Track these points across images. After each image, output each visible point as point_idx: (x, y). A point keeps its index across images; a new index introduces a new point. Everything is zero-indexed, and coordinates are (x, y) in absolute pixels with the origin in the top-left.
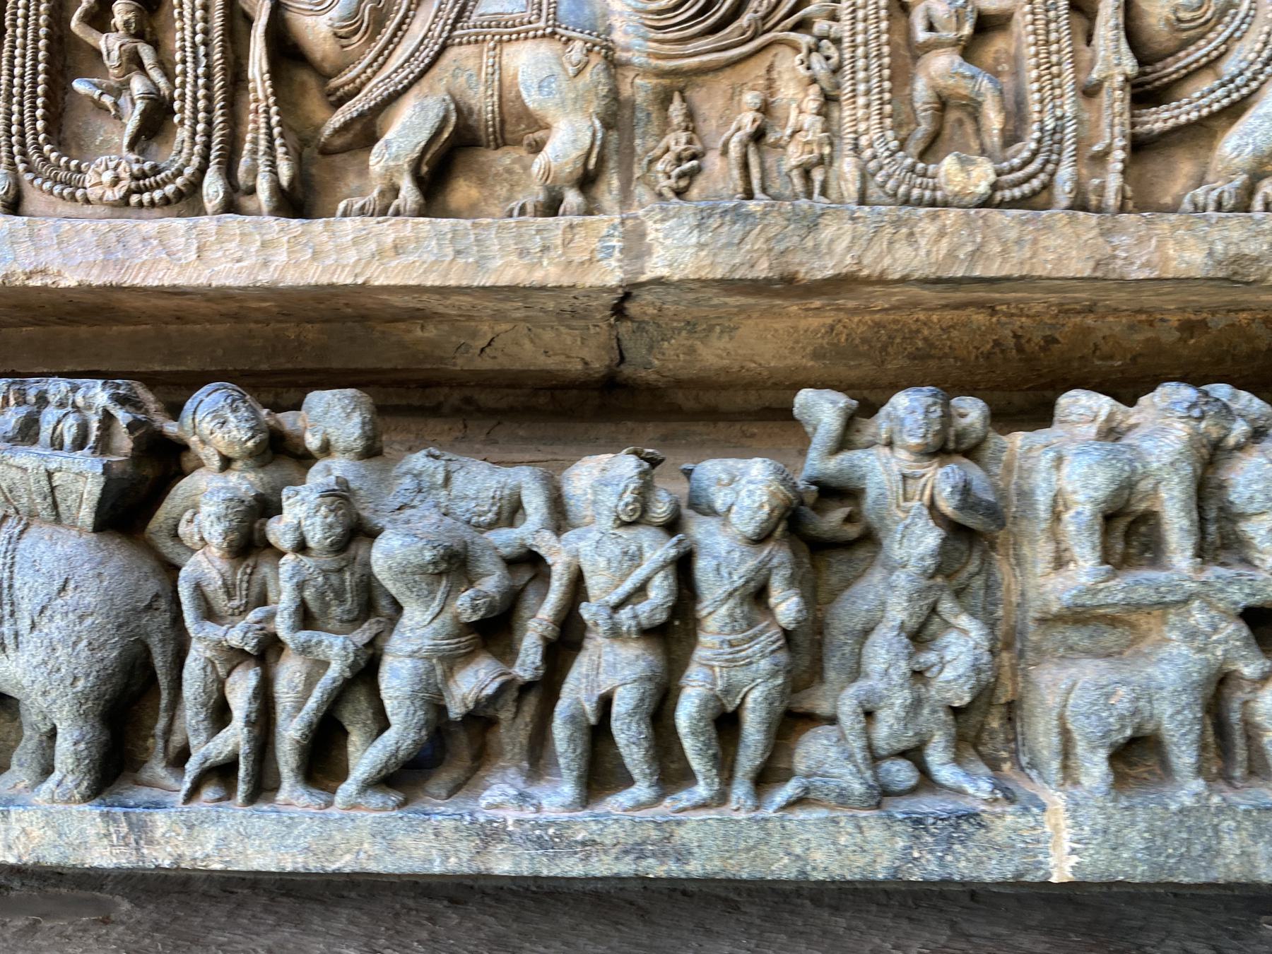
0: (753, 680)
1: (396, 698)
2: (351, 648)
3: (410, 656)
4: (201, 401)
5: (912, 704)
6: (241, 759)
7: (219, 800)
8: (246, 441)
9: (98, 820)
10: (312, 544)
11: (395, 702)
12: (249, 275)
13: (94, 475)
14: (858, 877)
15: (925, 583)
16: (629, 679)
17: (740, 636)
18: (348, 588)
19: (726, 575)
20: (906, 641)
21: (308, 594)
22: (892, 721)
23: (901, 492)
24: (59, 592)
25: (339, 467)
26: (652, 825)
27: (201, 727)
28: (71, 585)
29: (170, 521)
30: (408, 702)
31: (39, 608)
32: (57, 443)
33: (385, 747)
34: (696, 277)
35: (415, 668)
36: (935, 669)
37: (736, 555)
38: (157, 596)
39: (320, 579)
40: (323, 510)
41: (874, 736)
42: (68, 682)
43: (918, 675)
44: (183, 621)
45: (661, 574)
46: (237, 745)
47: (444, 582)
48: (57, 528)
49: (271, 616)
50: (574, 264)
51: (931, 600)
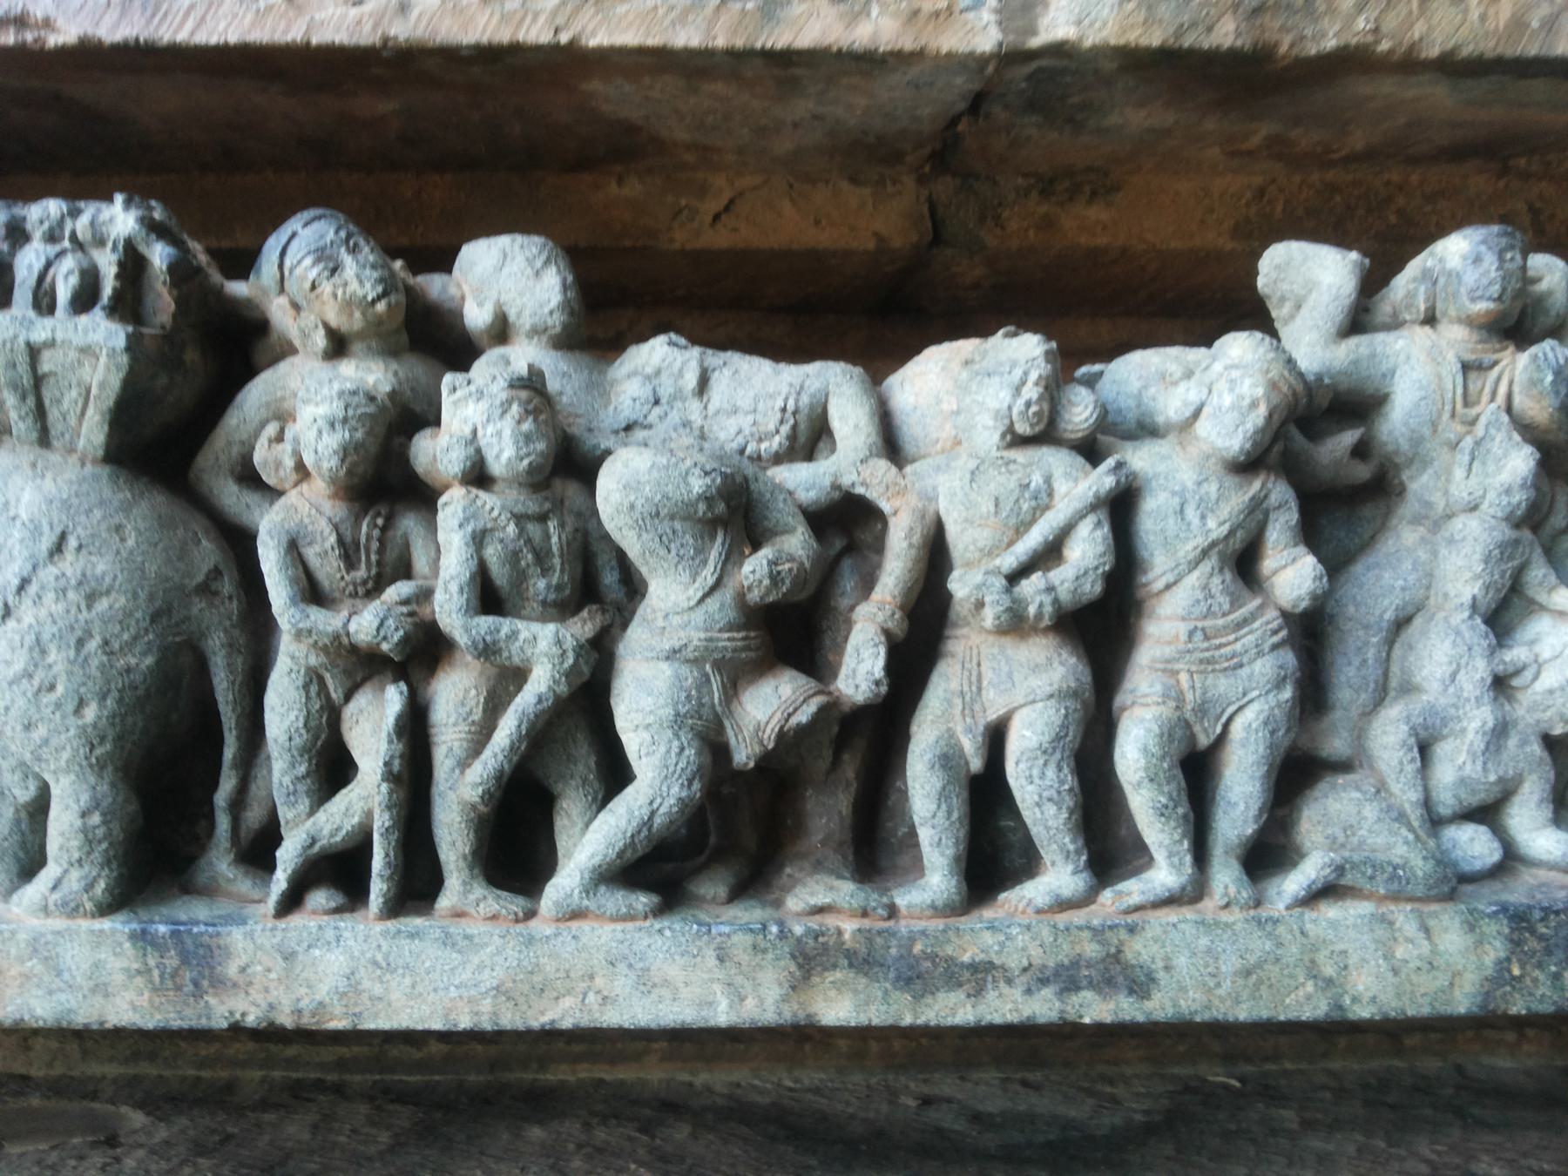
0: (1244, 694)
1: (648, 726)
2: (569, 643)
3: (667, 658)
4: (294, 235)
5: (1494, 730)
6: (376, 837)
7: (338, 910)
8: (374, 302)
9: (127, 945)
10: (497, 467)
11: (646, 736)
12: (376, 26)
13: (112, 353)
14: (1425, 1011)
15: (1509, 533)
16: (1040, 694)
17: (1220, 622)
18: (555, 549)
19: (1196, 522)
20: (1483, 627)
21: (492, 553)
22: (1462, 758)
23: (1459, 391)
24: (51, 555)
25: (523, 355)
26: (1086, 934)
27: (301, 788)
28: (72, 542)
29: (235, 450)
30: (669, 733)
31: (16, 582)
32: (44, 302)
33: (630, 812)
34: (1122, 42)
35: (677, 677)
36: (1528, 674)
37: (1212, 488)
38: (216, 573)
39: (511, 529)
40: (515, 408)
41: (1433, 783)
42: (70, 707)
43: (1501, 685)
44: (267, 605)
45: (1090, 520)
46: (369, 814)
47: (719, 539)
48: (45, 453)
49: (426, 595)
50: (922, 17)
51: (1516, 563)
